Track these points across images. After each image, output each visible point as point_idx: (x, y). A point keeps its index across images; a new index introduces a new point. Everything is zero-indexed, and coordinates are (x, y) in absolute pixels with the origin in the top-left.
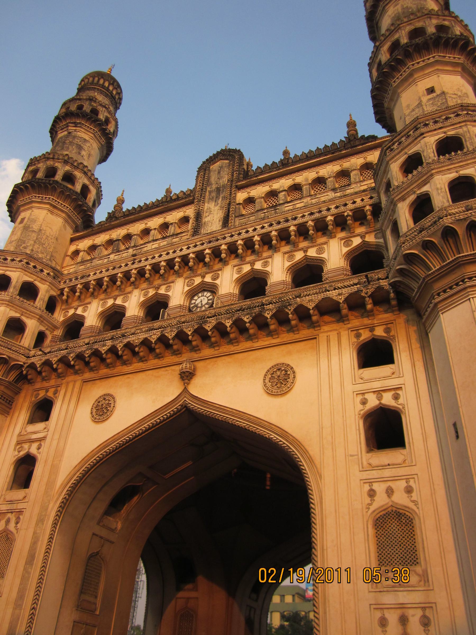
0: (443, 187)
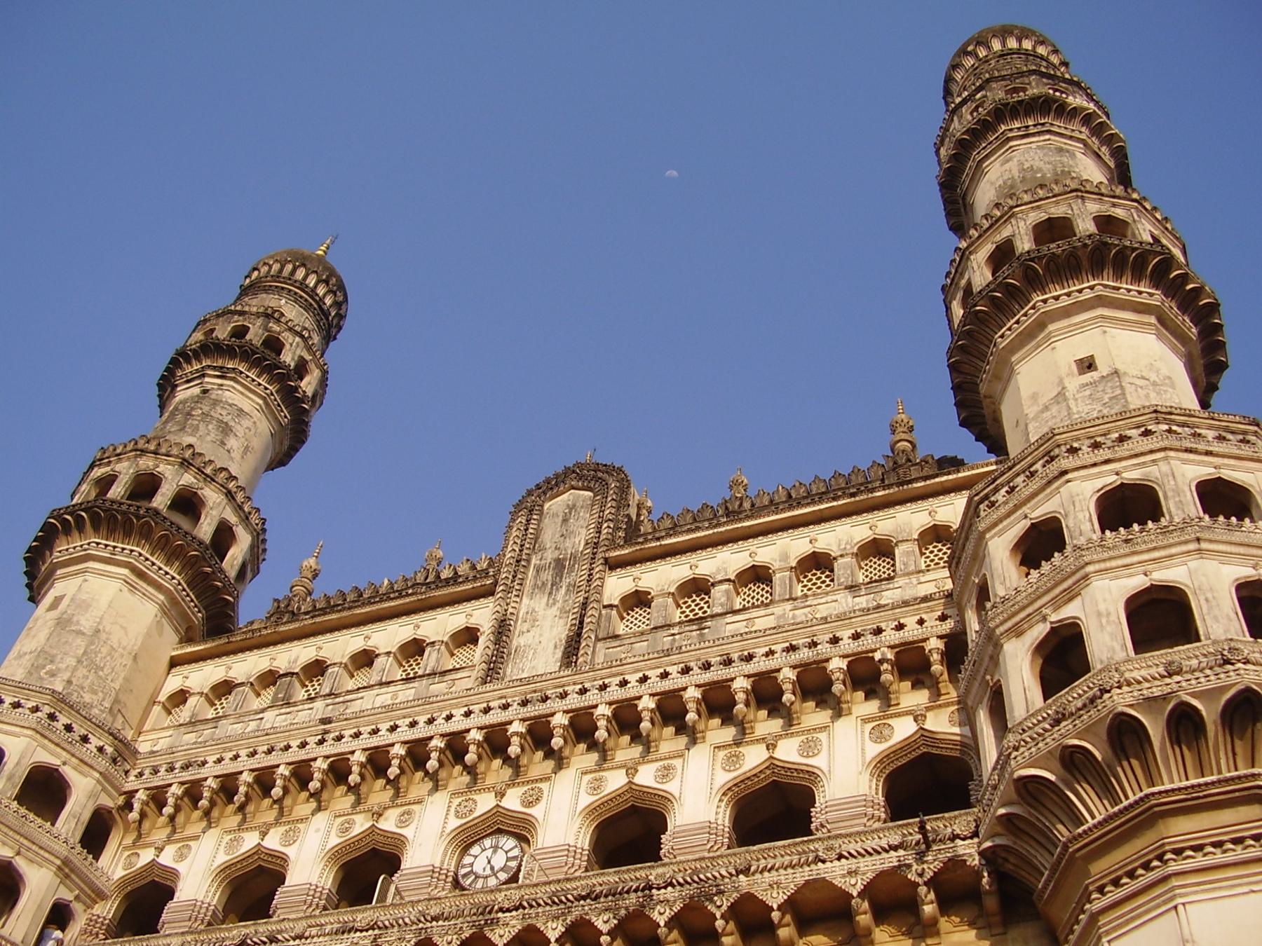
0: (1112, 610)
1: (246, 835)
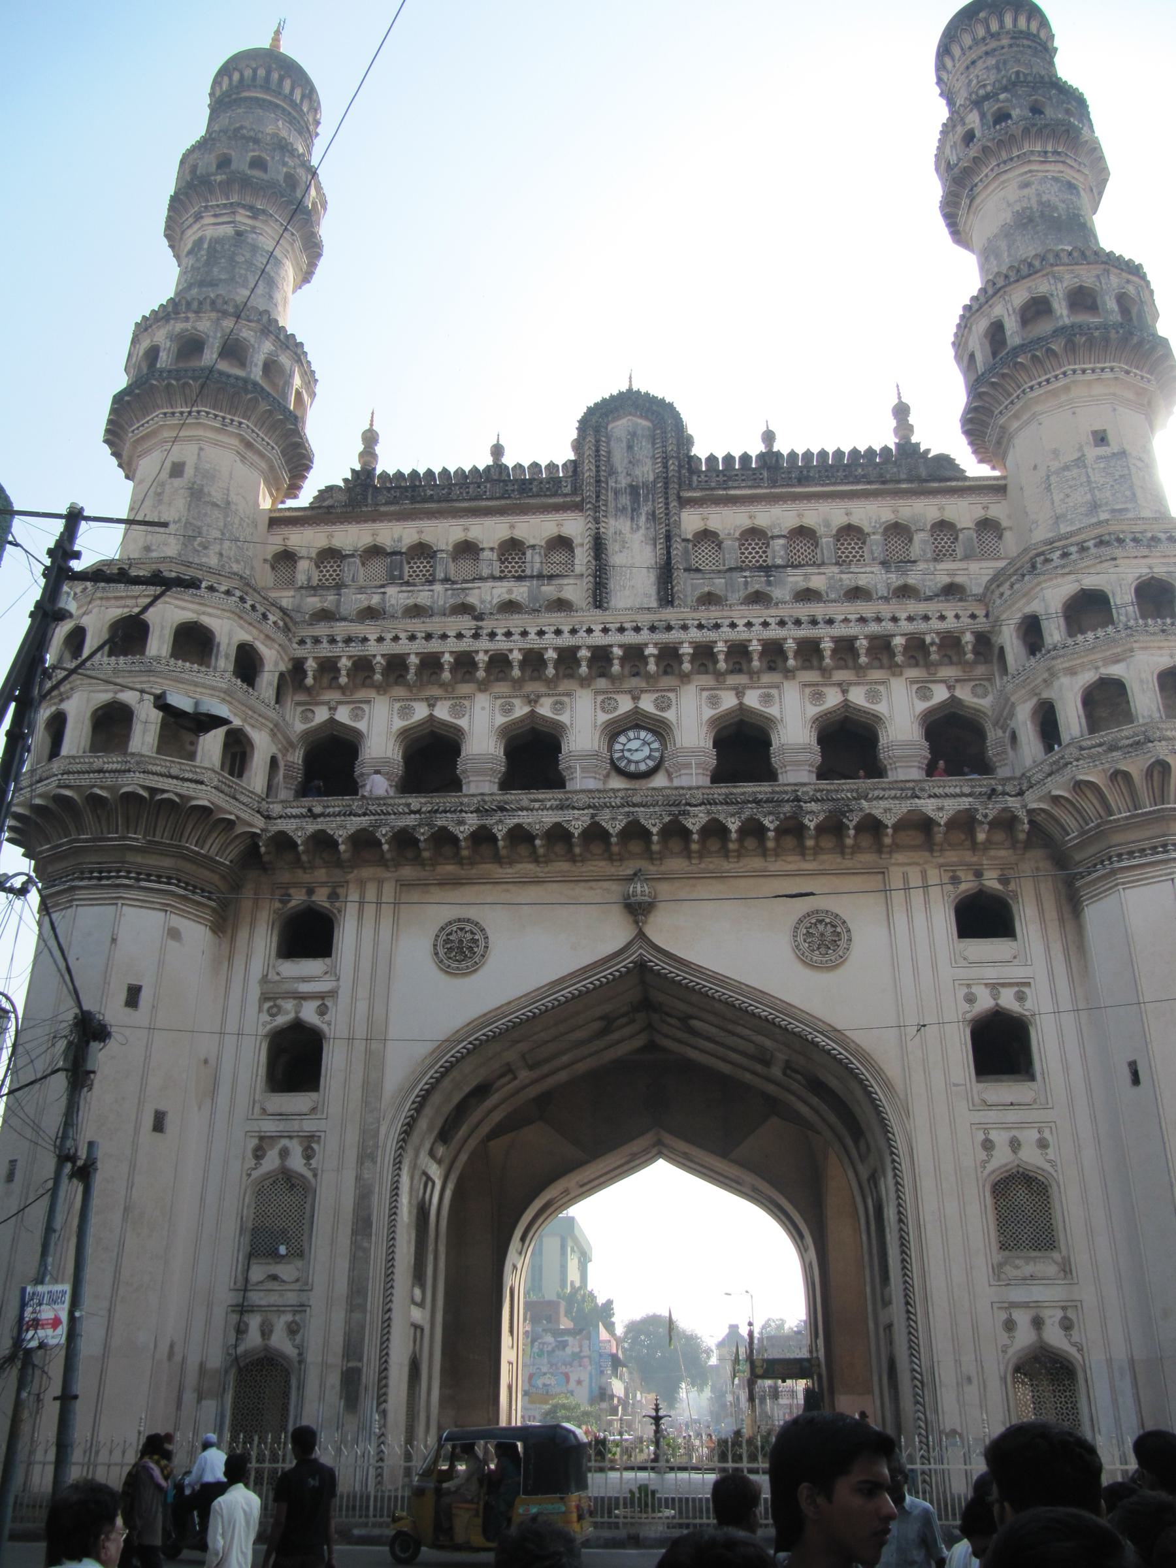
1: (414, 704)
